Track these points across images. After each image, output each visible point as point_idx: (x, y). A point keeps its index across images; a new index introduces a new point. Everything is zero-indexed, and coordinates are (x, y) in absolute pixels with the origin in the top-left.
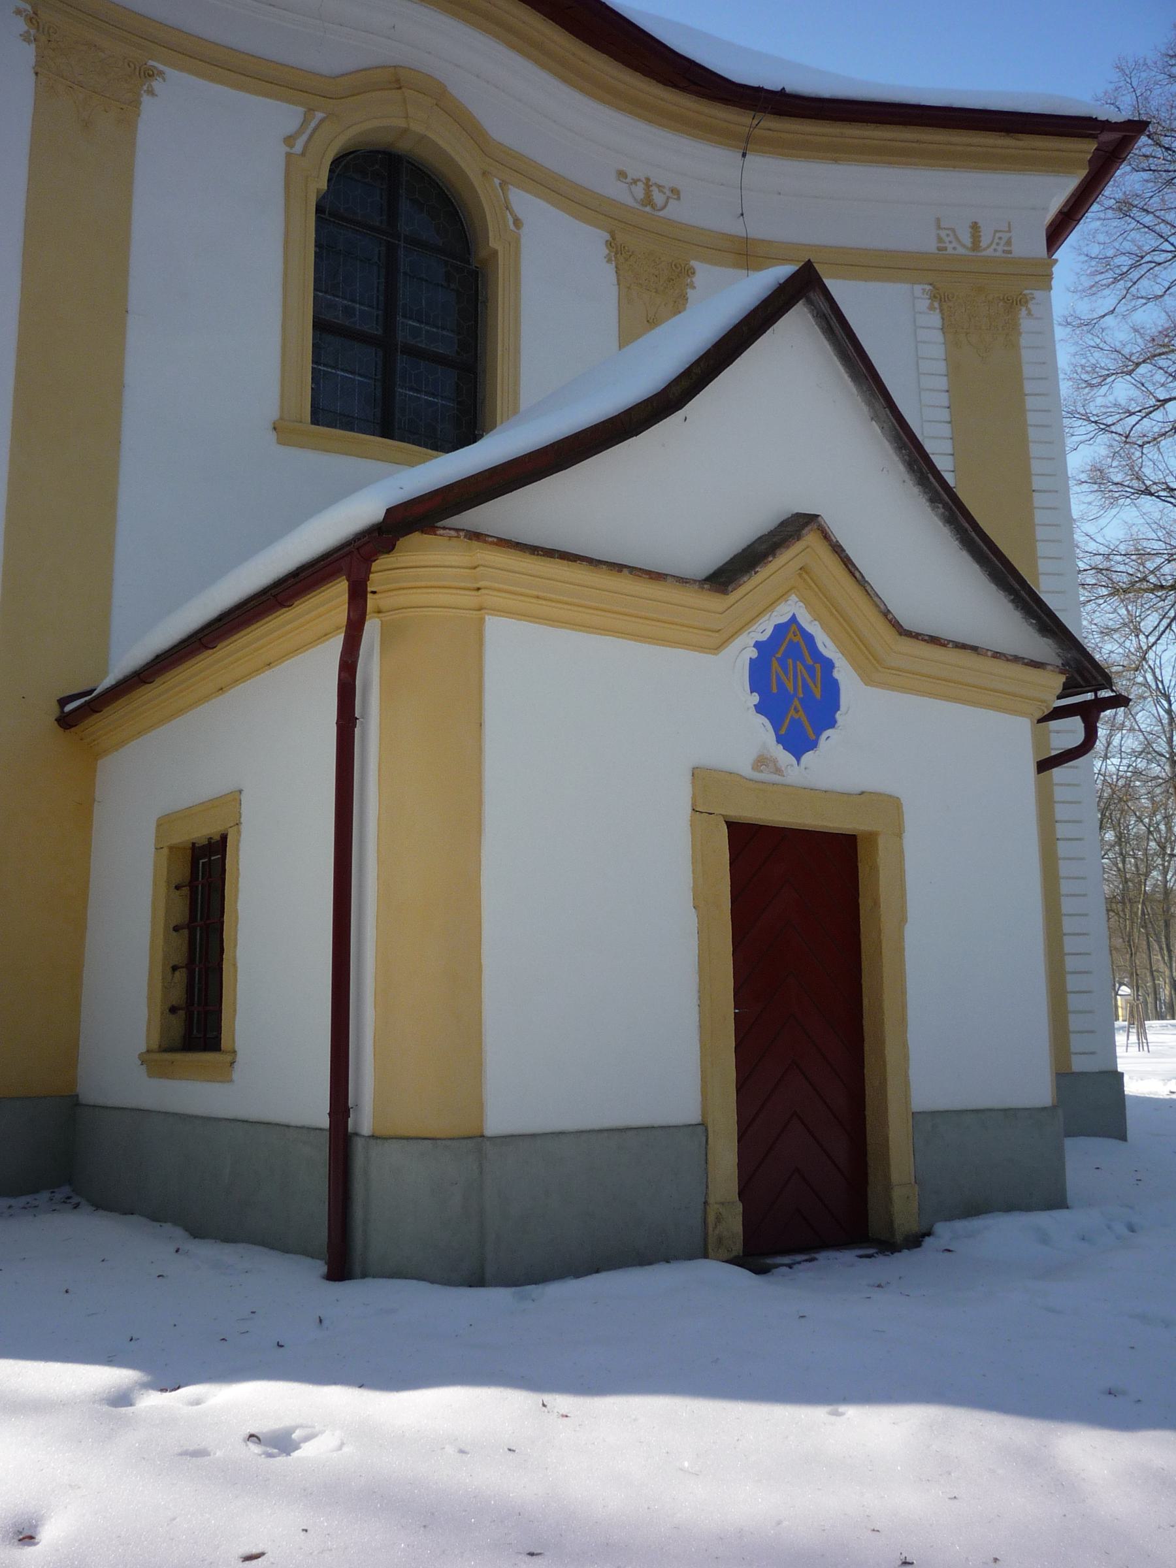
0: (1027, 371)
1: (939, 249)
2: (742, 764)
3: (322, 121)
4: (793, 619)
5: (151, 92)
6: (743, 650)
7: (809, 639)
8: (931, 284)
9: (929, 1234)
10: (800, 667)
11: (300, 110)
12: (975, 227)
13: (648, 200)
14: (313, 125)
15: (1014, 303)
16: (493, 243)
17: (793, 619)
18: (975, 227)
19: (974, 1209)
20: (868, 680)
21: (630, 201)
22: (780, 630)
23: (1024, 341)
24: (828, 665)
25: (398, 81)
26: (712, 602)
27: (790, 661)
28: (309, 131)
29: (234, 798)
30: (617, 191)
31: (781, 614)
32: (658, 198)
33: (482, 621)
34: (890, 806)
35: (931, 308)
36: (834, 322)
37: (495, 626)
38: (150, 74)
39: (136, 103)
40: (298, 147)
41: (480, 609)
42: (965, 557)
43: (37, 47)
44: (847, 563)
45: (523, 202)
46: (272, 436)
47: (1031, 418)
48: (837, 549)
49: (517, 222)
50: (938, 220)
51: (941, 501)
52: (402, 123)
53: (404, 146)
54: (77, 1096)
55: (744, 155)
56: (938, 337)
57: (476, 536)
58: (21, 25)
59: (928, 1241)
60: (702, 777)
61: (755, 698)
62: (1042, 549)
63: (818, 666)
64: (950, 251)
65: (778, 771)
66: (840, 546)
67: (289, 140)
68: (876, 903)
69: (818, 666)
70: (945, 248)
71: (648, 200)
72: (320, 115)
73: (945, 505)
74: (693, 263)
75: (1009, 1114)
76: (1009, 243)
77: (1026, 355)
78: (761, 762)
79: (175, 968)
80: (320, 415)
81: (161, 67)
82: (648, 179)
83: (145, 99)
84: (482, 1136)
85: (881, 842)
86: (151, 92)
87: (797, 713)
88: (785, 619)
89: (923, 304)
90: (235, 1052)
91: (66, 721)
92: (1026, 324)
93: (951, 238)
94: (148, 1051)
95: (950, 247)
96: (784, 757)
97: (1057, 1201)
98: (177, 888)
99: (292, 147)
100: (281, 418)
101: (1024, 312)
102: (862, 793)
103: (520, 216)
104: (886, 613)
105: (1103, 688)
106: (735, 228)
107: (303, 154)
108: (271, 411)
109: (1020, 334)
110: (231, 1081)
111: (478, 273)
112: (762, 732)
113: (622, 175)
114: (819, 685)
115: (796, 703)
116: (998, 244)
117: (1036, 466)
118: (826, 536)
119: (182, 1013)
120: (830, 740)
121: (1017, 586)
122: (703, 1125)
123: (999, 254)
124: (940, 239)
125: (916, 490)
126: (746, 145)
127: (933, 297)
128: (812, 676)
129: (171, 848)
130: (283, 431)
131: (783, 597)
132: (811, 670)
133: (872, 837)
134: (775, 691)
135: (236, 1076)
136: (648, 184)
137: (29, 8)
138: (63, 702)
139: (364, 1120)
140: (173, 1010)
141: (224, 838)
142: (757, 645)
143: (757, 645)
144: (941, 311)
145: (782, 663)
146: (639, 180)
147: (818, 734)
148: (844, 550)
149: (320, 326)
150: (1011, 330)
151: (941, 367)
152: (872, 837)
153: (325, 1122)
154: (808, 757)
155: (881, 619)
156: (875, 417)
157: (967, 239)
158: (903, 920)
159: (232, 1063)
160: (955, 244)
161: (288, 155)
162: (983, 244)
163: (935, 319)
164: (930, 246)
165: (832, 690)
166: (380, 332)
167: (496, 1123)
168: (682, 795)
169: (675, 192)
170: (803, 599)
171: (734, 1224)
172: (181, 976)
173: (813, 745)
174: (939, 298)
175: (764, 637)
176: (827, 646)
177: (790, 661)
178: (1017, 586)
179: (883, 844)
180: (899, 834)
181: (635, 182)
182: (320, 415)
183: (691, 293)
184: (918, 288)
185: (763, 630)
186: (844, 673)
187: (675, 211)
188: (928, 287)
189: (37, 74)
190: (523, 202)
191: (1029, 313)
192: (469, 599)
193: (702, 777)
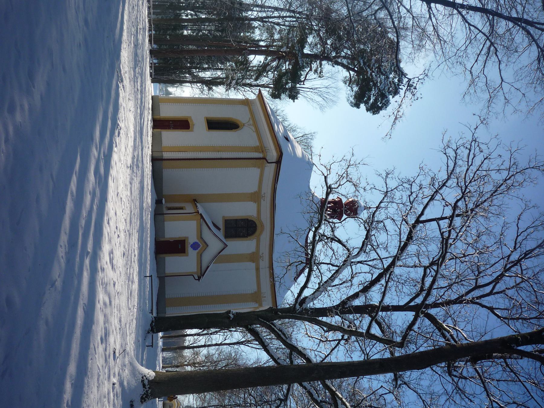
6: (197, 241)
29: (185, 209)
31: (201, 245)
32: (262, 258)
60: (188, 238)
78: (190, 243)
91: (195, 200)
112: (192, 243)
113: (263, 253)
130: (223, 217)
139: (165, 215)
163: (253, 292)
167: (165, 223)
169: (263, 260)
173: (192, 248)
174: (256, 292)
176: (199, 249)
179: (184, 254)
185: (199, 243)
186: (197, 251)
187: (261, 260)
193: (188, 238)
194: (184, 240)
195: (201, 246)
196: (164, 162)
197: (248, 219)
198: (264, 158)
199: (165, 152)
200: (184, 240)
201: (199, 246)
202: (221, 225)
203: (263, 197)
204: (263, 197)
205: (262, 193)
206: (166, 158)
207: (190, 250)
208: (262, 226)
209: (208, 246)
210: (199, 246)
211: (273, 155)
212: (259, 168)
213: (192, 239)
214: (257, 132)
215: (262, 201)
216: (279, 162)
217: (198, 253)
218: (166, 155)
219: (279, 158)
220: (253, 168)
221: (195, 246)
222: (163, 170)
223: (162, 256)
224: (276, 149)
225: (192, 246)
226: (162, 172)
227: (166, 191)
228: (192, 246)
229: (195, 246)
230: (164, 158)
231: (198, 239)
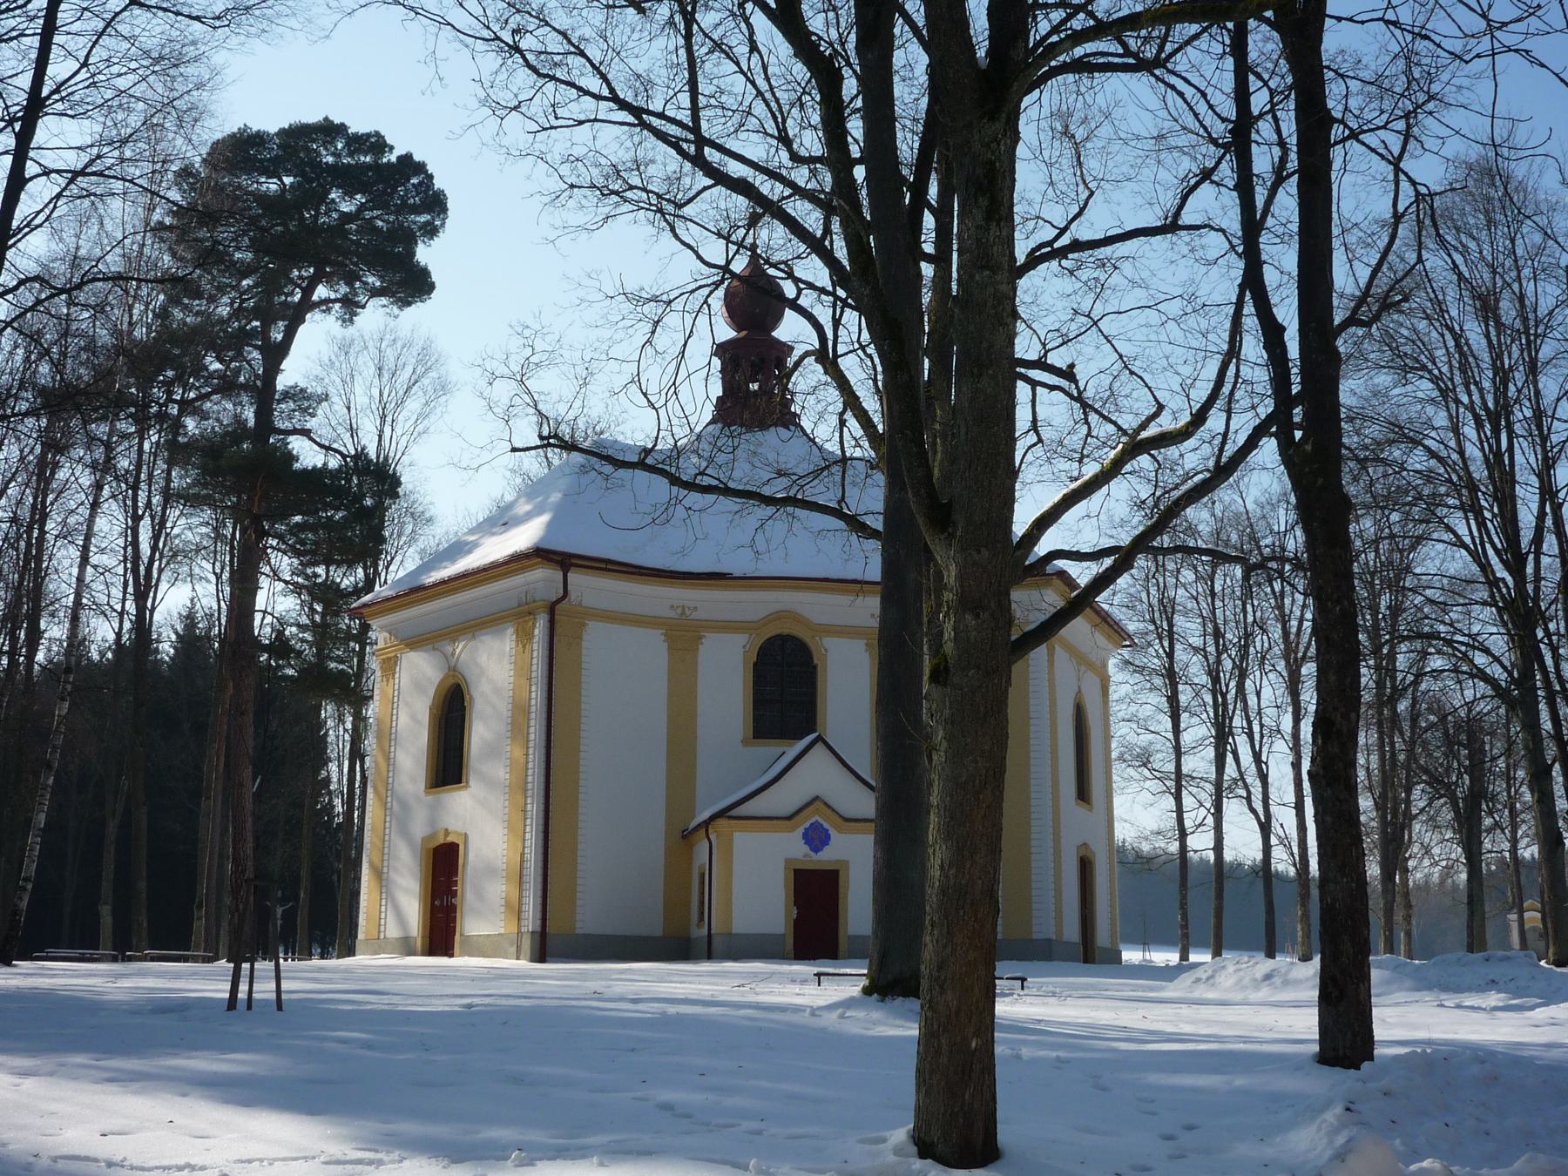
6: (801, 830)
38: (701, 638)
45: (829, 642)
60: (788, 861)
91: (684, 837)
96: (812, 854)
104: (840, 816)
108: (740, 736)
112: (806, 849)
120: (827, 849)
130: (745, 742)
165: (828, 837)
168: (782, 865)
176: (826, 825)
185: (807, 825)
186: (832, 832)
193: (788, 861)
194: (795, 870)
197: (755, 664)
198: (552, 609)
200: (795, 870)
201: (816, 827)
202: (768, 750)
203: (683, 613)
204: (683, 613)
205: (672, 614)
206: (539, 922)
207: (828, 856)
208: (779, 616)
209: (817, 798)
210: (816, 827)
211: (542, 578)
212: (584, 625)
213: (791, 846)
214: (471, 627)
215: (695, 615)
216: (564, 561)
218: (531, 921)
219: (551, 560)
220: (584, 644)
221: (817, 838)
222: (579, 931)
223: (843, 944)
224: (523, 570)
225: (816, 850)
226: (586, 936)
227: (653, 925)
228: (816, 850)
229: (817, 838)
231: (793, 829)
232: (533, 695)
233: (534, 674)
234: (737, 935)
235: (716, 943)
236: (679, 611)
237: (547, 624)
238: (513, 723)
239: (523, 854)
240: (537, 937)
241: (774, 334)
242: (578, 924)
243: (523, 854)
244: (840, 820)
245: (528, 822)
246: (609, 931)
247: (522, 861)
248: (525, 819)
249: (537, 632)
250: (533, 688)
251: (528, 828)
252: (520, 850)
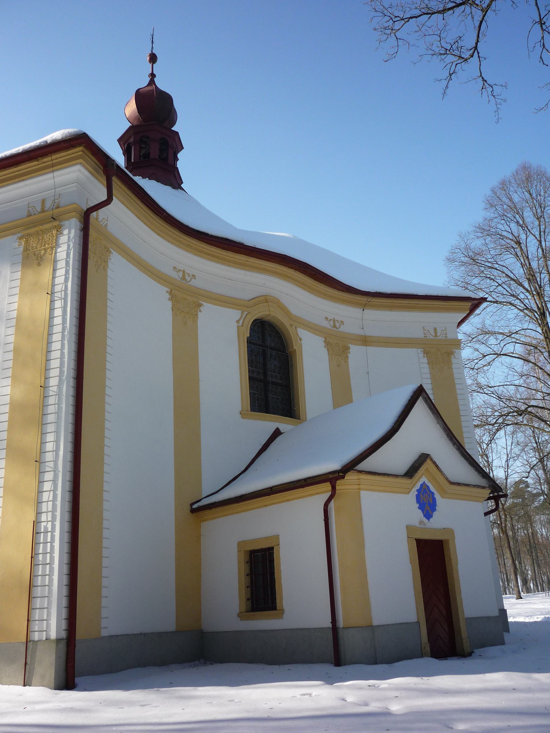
0: (456, 376)
1: (424, 337)
2: (417, 524)
3: (247, 315)
4: (424, 482)
5: (200, 311)
6: (414, 493)
7: (428, 487)
8: (423, 349)
9: (473, 652)
10: (427, 495)
11: (240, 312)
12: (435, 329)
13: (335, 326)
14: (244, 316)
15: (450, 354)
16: (295, 348)
17: (424, 482)
18: (435, 329)
19: (483, 646)
20: (443, 497)
21: (329, 327)
22: (422, 485)
23: (454, 366)
24: (433, 494)
25: (266, 300)
26: (406, 481)
27: (424, 494)
28: (243, 318)
29: (277, 537)
30: (326, 324)
31: (421, 482)
32: (337, 325)
33: (359, 492)
34: (451, 532)
35: (424, 356)
36: (428, 400)
37: (363, 493)
38: (200, 305)
39: (197, 315)
40: (240, 324)
41: (359, 489)
42: (463, 459)
43: (172, 302)
44: (437, 466)
46: (240, 416)
47: (458, 392)
48: (434, 463)
49: (300, 339)
50: (424, 327)
51: (456, 444)
52: (268, 313)
53: (267, 319)
54: (202, 630)
55: (363, 310)
56: (427, 366)
57: (360, 472)
58: (168, 296)
59: (473, 654)
60: (409, 528)
61: (418, 505)
62: (465, 435)
63: (431, 494)
64: (428, 337)
65: (425, 524)
66: (435, 462)
67: (238, 321)
68: (450, 559)
69: (431, 494)
70: (427, 337)
71: (335, 326)
72: (246, 313)
73: (457, 446)
74: (350, 345)
75: (488, 618)
76: (446, 334)
77: (455, 371)
78: (421, 522)
79: (247, 587)
80: (253, 409)
81: (202, 303)
82: (334, 319)
83: (199, 313)
84: (372, 626)
85: (450, 541)
86: (200, 311)
87: (427, 508)
88: (422, 483)
89: (421, 355)
90: (284, 610)
91: (193, 511)
92: (454, 361)
93: (428, 333)
94: (240, 613)
95: (428, 336)
96: (425, 520)
97: (503, 643)
98: (247, 563)
99: (238, 324)
100: (242, 410)
101: (453, 357)
102: (444, 529)
103: (301, 337)
104: (447, 479)
105: (500, 492)
106: (361, 332)
107: (242, 326)
108: (240, 409)
109: (452, 364)
110: (283, 618)
111: (288, 356)
112: (419, 514)
113: (326, 318)
114: (431, 498)
115: (427, 505)
116: (443, 335)
117: (461, 408)
118: (432, 460)
119: (250, 600)
120: (435, 514)
121: (476, 466)
122: (418, 622)
123: (443, 338)
124: (425, 334)
125: (449, 442)
126: (364, 307)
127: (424, 353)
128: (430, 497)
129: (245, 551)
130: (243, 414)
131: (421, 477)
132: (429, 495)
133: (447, 541)
134: (422, 502)
135: (284, 616)
136: (334, 320)
137: (169, 290)
138: (192, 505)
139: (341, 623)
140: (248, 600)
141: (272, 549)
142: (417, 490)
143: (417, 490)
144: (427, 357)
145: (423, 494)
146: (331, 319)
147: (432, 513)
148: (436, 463)
149: (250, 378)
150: (449, 363)
151: (428, 376)
152: (447, 541)
153: (330, 625)
154: (431, 520)
155: (446, 480)
156: (438, 423)
157: (433, 334)
158: (457, 564)
159: (283, 613)
160: (429, 335)
161: (238, 326)
162: (438, 334)
163: (425, 360)
164: (422, 336)
165: (434, 500)
166: (262, 378)
167: (375, 623)
169: (342, 322)
170: (426, 477)
171: (428, 649)
172: (249, 589)
174: (426, 353)
175: (418, 488)
176: (432, 489)
177: (424, 494)
178: (476, 466)
179: (451, 542)
180: (454, 539)
181: (330, 320)
182: (253, 409)
183: (349, 355)
184: (419, 350)
185: (418, 486)
186: (437, 496)
187: (342, 329)
188: (422, 350)
189: (173, 310)
190: (303, 333)
191: (454, 357)
192: (357, 487)
193: (409, 528)
195: (424, 479)
196: (80, 634)
199: (36, 627)
204: (184, 278)
206: (64, 625)
208: (266, 299)
215: (194, 283)
217: (445, 493)
220: (109, 273)
222: (104, 633)
223: (464, 631)
224: (53, 167)
225: (428, 516)
228: (428, 516)
230: (64, 635)
232: (58, 312)
233: (58, 288)
234: (378, 626)
235: (346, 640)
236: (181, 274)
237: (80, 234)
238: (16, 351)
239: (36, 523)
240: (63, 646)
241: (174, 129)
242: (104, 623)
243: (36, 523)
244: (447, 484)
245: (48, 476)
246: (129, 632)
247: (36, 533)
248: (41, 473)
249: (63, 239)
250: (58, 304)
251: (47, 486)
252: (32, 517)
